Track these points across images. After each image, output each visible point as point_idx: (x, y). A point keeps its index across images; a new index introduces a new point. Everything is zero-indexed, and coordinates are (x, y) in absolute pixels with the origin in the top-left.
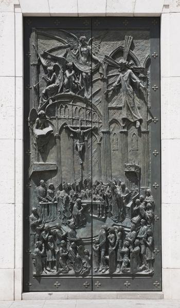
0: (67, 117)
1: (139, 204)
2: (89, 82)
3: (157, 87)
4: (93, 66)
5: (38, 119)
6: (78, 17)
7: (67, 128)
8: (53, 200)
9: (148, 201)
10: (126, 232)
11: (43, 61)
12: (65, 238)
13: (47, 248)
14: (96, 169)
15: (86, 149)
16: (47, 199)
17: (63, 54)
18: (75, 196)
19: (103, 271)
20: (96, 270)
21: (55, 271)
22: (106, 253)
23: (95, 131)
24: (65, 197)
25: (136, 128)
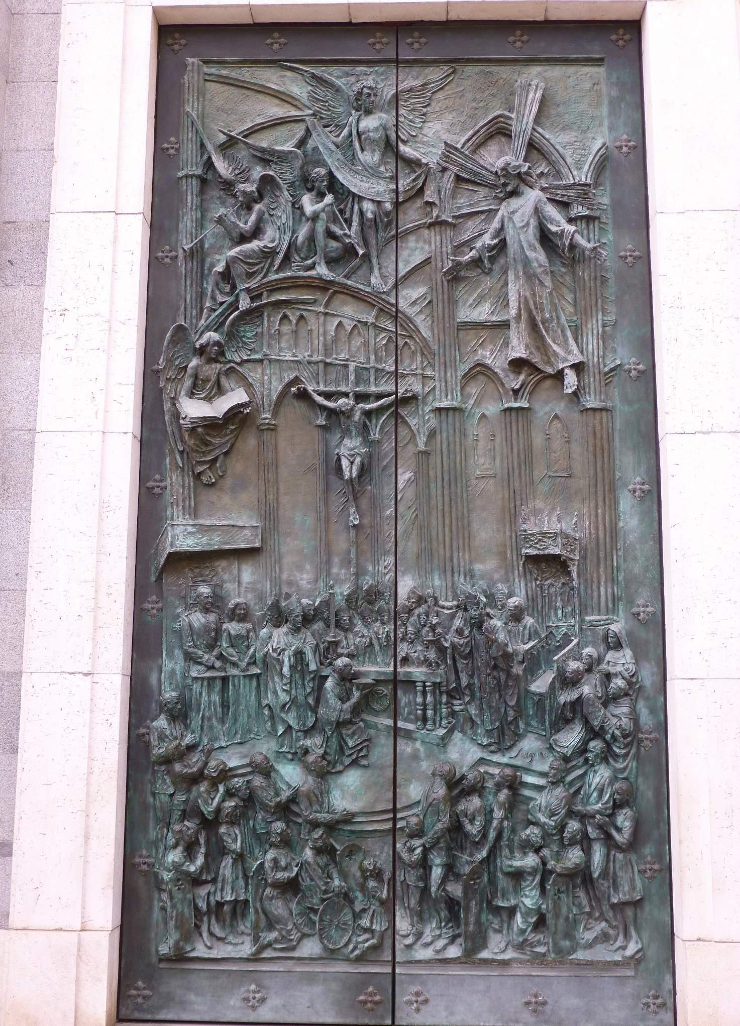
0: (303, 355)
3: (636, 254)
4: (401, 183)
5: (194, 362)
6: (350, 24)
7: (303, 395)
8: (243, 664)
9: (612, 670)
10: (527, 793)
11: (221, 166)
12: (286, 810)
13: (217, 851)
14: (410, 547)
15: (376, 472)
16: (220, 657)
17: (295, 141)
18: (327, 649)
19: (441, 943)
20: (408, 941)
21: (248, 940)
23: (410, 400)
24: (289, 652)
25: (563, 396)
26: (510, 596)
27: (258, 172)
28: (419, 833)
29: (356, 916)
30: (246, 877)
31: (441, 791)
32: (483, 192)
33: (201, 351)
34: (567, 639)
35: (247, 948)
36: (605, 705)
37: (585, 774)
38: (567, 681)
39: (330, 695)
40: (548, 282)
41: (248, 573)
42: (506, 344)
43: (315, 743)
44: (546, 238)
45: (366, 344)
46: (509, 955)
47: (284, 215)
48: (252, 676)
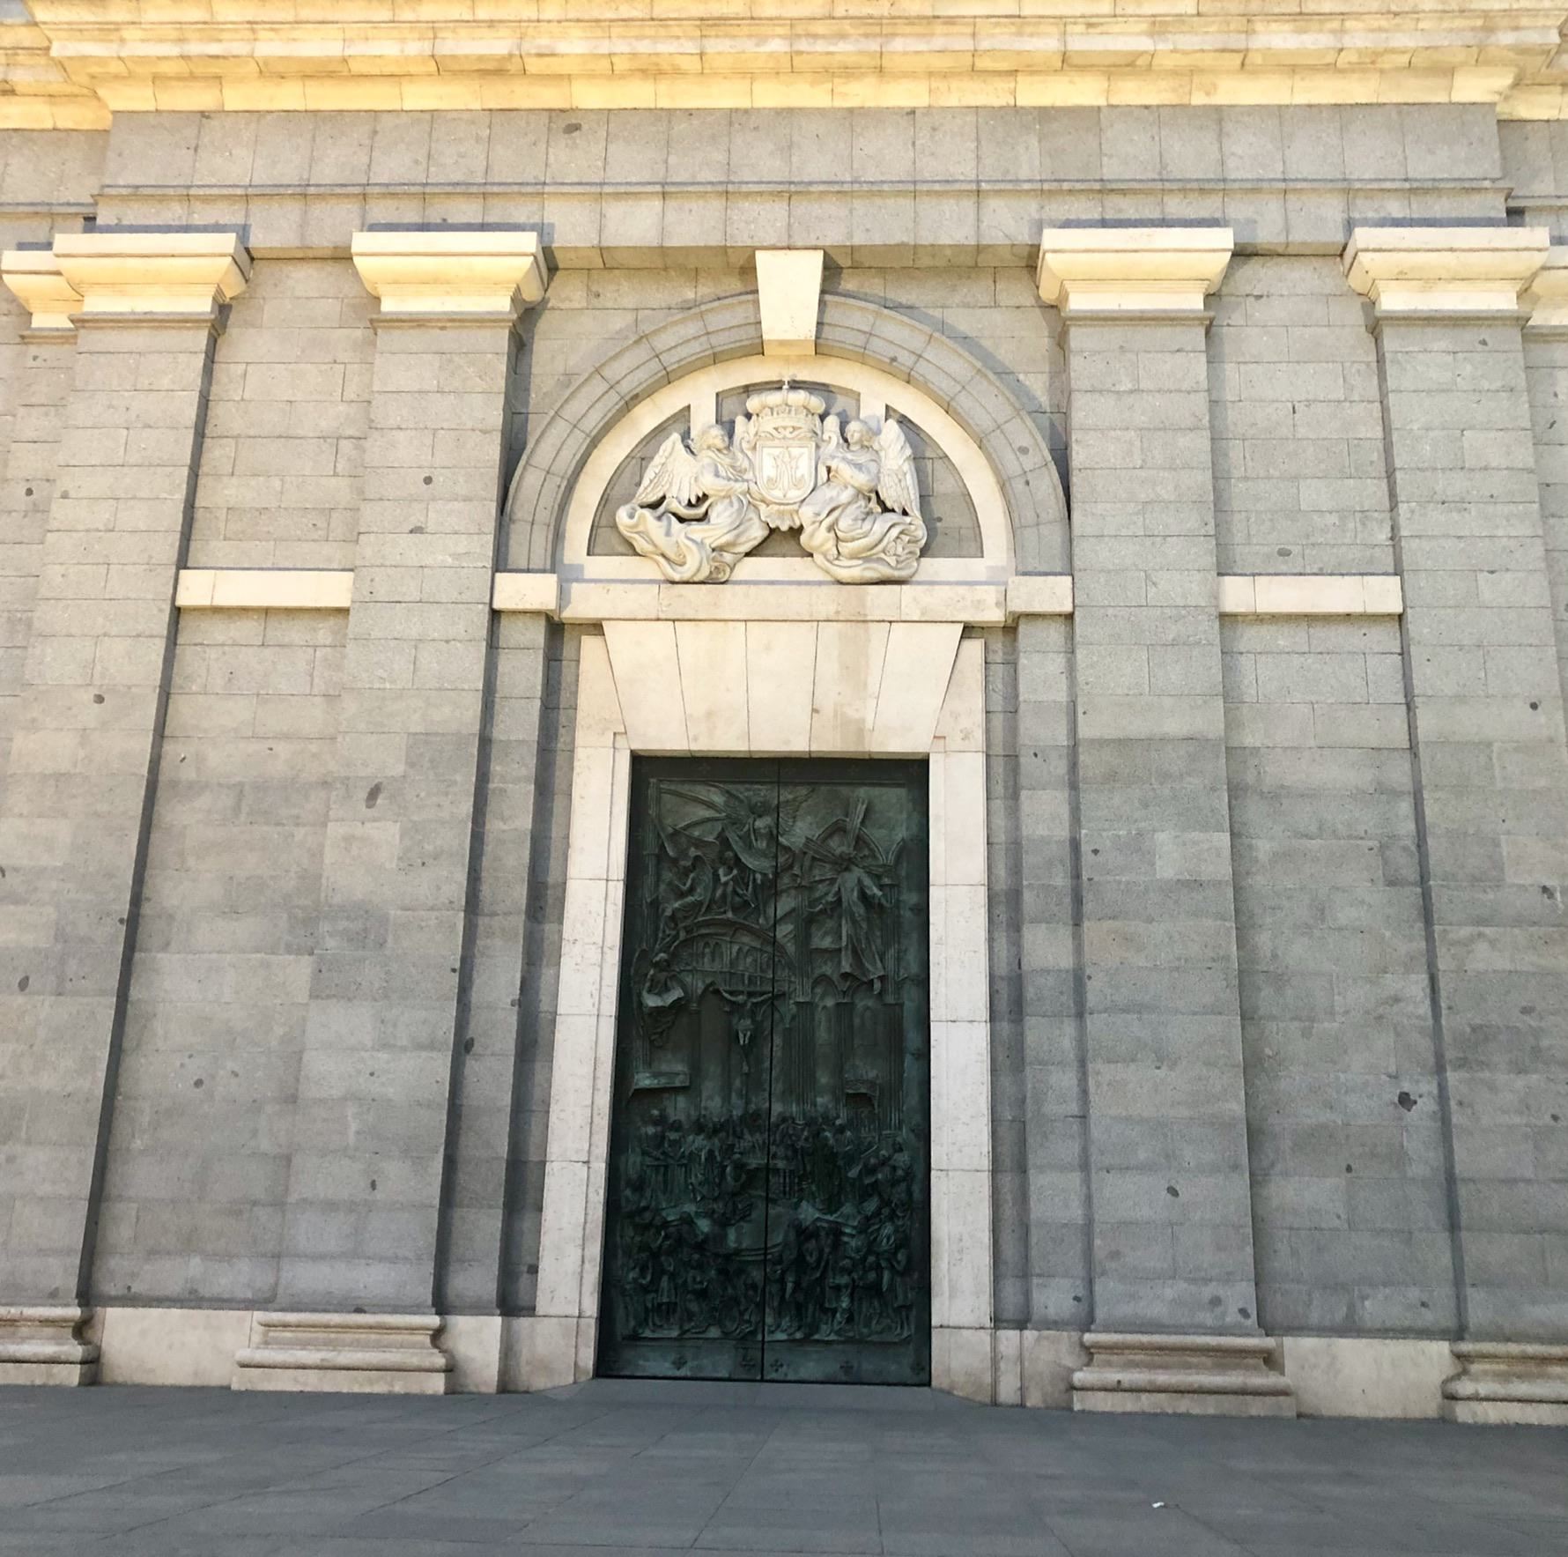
0: (717, 966)
1: (872, 1171)
2: (770, 889)
5: (652, 972)
7: (717, 992)
10: (846, 1239)
12: (700, 1246)
14: (778, 1088)
16: (664, 1153)
17: (716, 834)
22: (797, 1284)
26: (838, 1117)
27: (693, 852)
28: (780, 1262)
29: (742, 1314)
30: (676, 1289)
31: (792, 1236)
32: (828, 866)
33: (656, 965)
34: (870, 1145)
35: (675, 1334)
36: (893, 1185)
37: (879, 1229)
38: (872, 1171)
39: (729, 1178)
40: (864, 925)
41: (681, 1101)
42: (839, 963)
43: (719, 1207)
44: (864, 897)
45: (756, 961)
46: (833, 1337)
47: (707, 878)
48: (681, 1165)
